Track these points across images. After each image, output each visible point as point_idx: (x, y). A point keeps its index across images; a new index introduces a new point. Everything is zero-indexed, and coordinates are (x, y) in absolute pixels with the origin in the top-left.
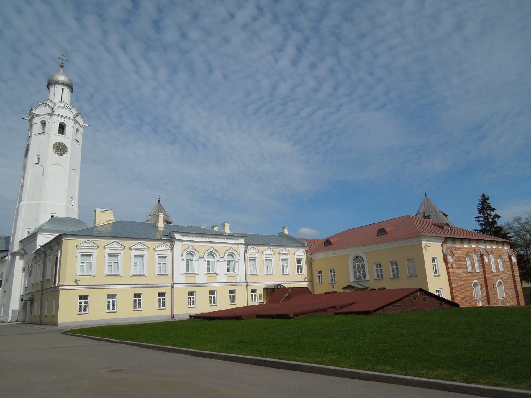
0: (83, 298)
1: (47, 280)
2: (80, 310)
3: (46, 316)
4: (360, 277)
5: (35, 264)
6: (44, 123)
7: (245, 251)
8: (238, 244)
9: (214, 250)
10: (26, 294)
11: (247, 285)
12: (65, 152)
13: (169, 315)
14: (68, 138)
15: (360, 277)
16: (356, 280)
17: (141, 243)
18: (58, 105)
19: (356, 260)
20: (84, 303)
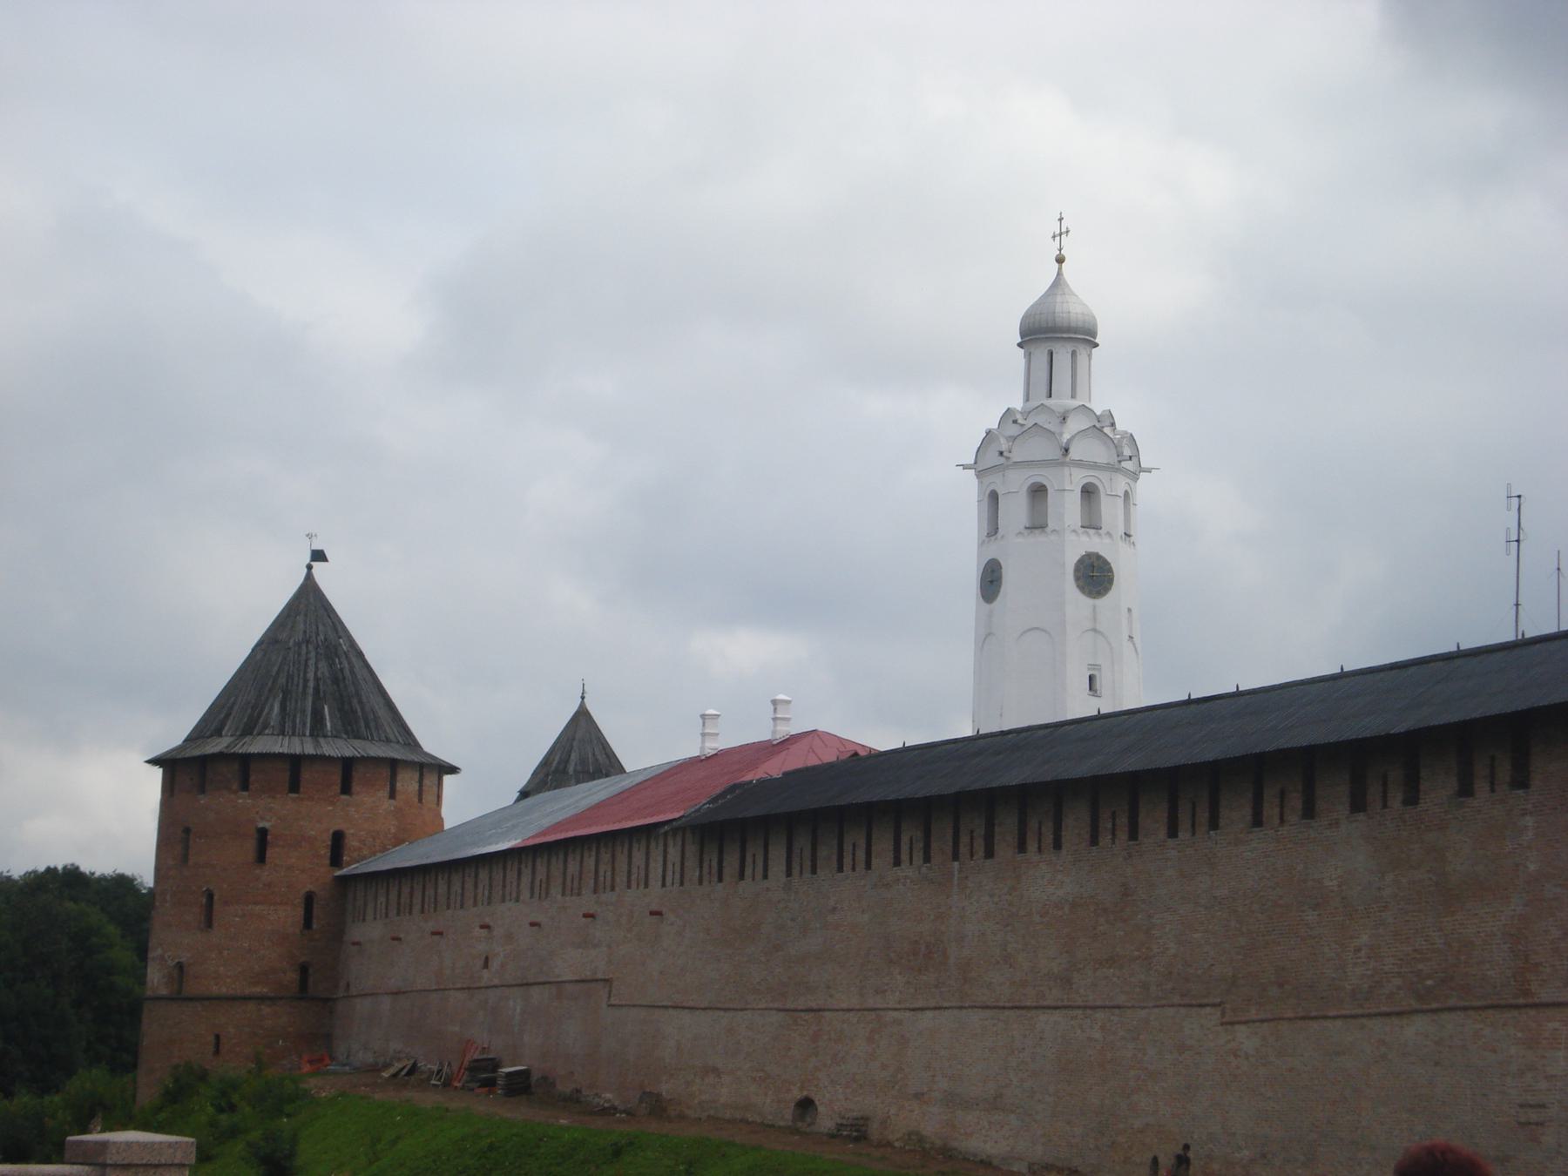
6: (1038, 492)
14: (1108, 534)
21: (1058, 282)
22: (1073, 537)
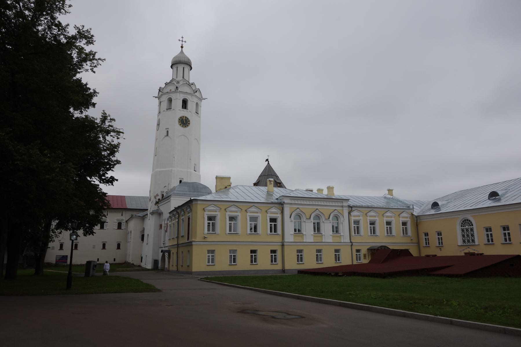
1: (181, 236)
2: (209, 262)
3: (182, 266)
4: (469, 241)
5: (170, 222)
6: (170, 100)
7: (349, 213)
8: (342, 206)
10: (164, 247)
11: (352, 245)
12: (188, 125)
13: (281, 270)
15: (469, 241)
16: (464, 244)
17: (255, 206)
18: (181, 83)
19: (464, 223)
20: (211, 257)
21: (182, 51)
22: (179, 111)
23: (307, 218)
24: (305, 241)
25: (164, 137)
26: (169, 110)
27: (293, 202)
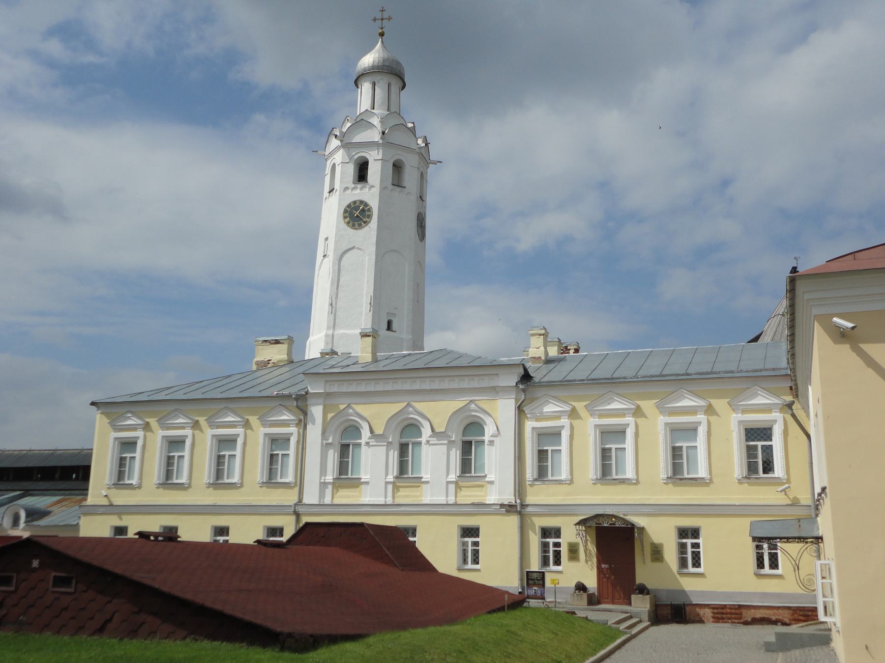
0: (690, 535)
7: (520, 409)
9: (355, 415)
13: (571, 587)
23: (437, 430)
24: (427, 500)
25: (323, 259)
26: (331, 194)
27: (335, 389)
